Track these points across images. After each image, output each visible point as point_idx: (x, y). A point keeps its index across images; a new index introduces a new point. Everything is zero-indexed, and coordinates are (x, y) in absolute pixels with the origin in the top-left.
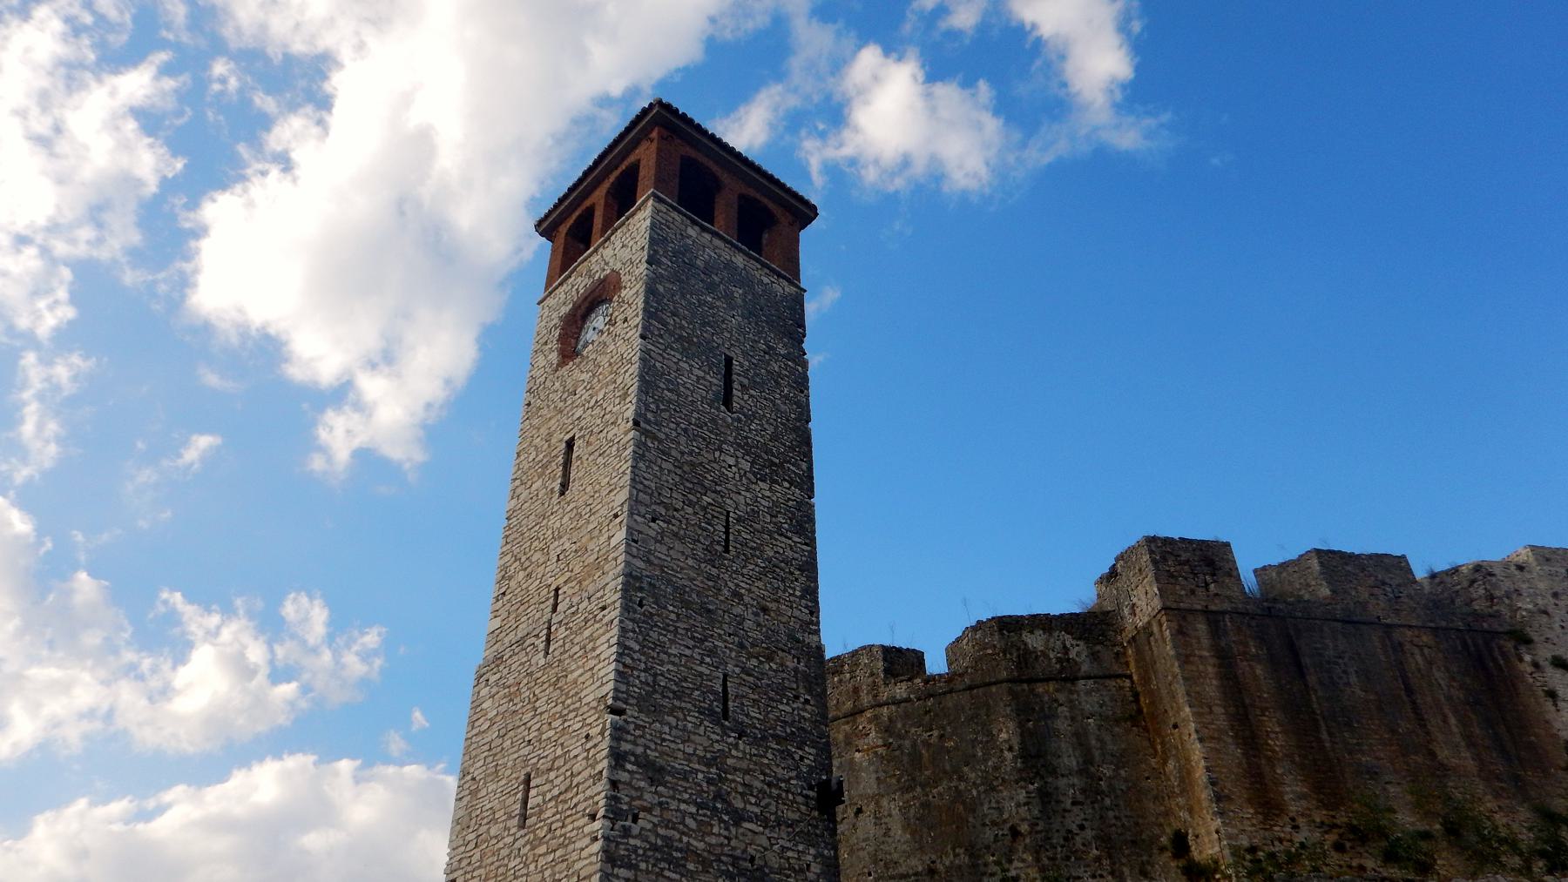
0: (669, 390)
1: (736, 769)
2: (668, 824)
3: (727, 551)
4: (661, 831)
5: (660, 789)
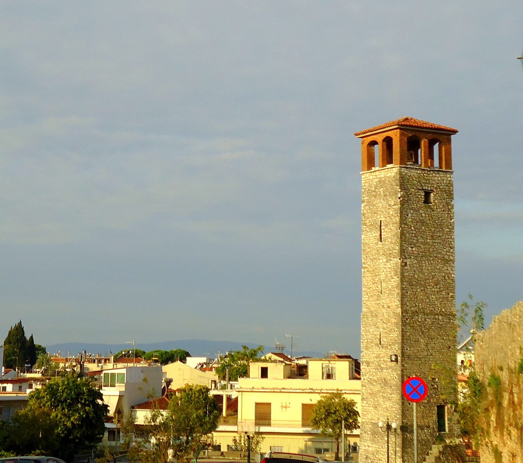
0: (368, 248)
1: (382, 357)
2: (371, 375)
3: (381, 293)
4: (370, 377)
5: (370, 367)
